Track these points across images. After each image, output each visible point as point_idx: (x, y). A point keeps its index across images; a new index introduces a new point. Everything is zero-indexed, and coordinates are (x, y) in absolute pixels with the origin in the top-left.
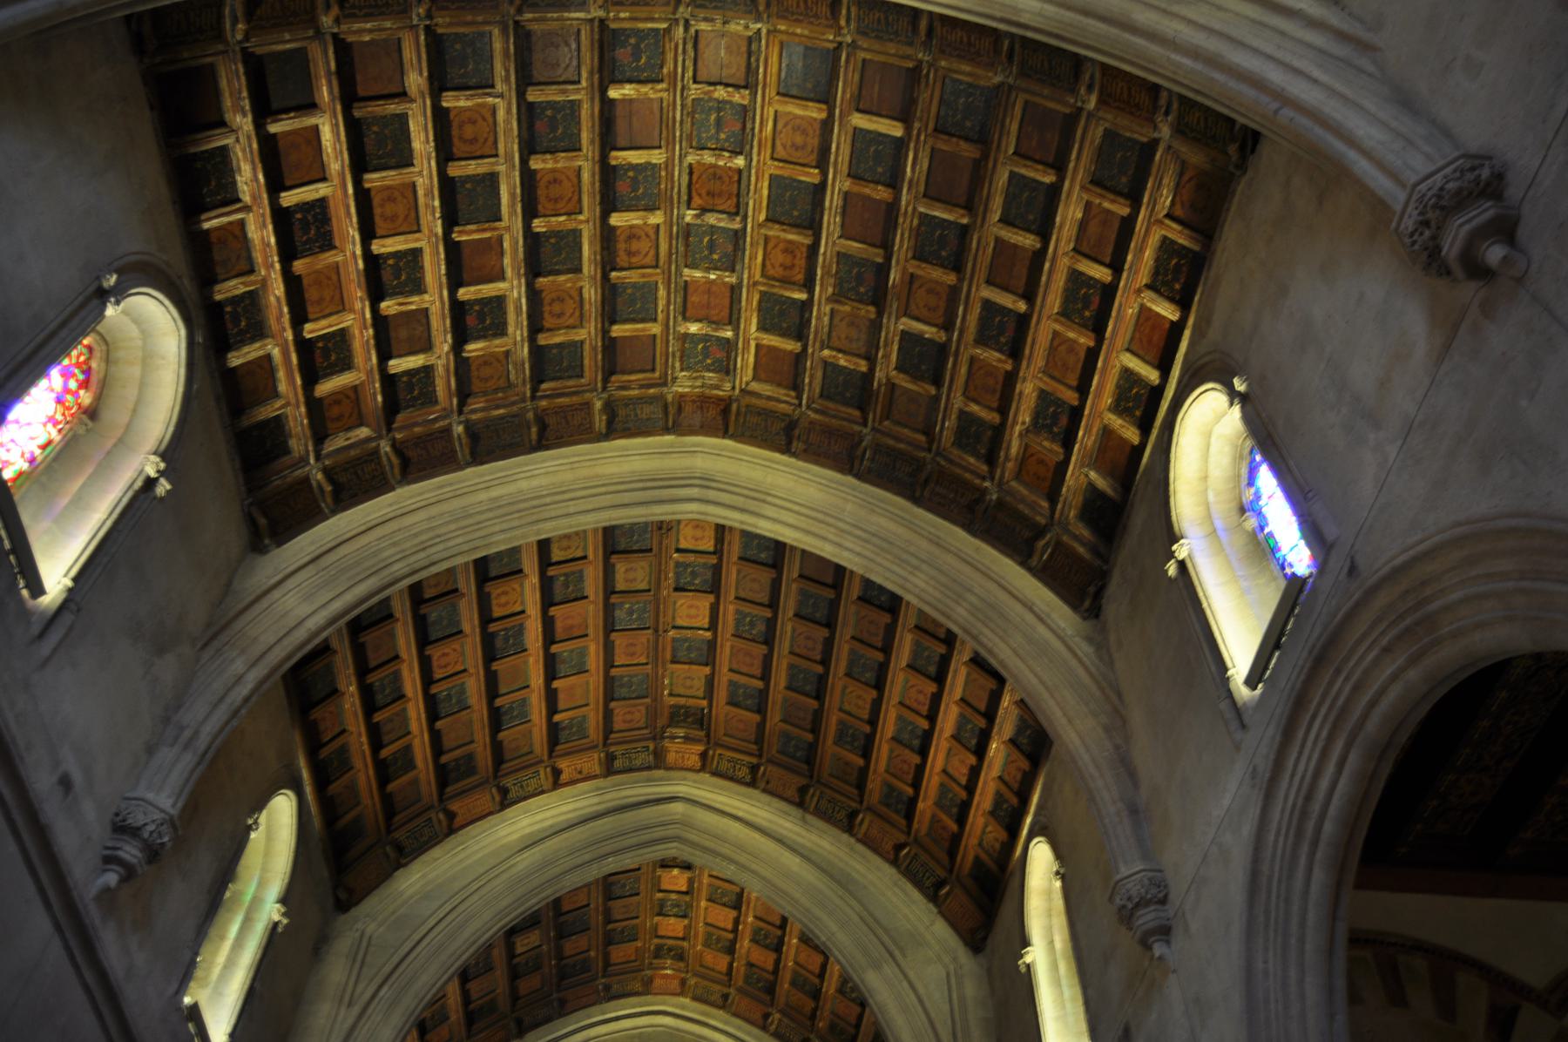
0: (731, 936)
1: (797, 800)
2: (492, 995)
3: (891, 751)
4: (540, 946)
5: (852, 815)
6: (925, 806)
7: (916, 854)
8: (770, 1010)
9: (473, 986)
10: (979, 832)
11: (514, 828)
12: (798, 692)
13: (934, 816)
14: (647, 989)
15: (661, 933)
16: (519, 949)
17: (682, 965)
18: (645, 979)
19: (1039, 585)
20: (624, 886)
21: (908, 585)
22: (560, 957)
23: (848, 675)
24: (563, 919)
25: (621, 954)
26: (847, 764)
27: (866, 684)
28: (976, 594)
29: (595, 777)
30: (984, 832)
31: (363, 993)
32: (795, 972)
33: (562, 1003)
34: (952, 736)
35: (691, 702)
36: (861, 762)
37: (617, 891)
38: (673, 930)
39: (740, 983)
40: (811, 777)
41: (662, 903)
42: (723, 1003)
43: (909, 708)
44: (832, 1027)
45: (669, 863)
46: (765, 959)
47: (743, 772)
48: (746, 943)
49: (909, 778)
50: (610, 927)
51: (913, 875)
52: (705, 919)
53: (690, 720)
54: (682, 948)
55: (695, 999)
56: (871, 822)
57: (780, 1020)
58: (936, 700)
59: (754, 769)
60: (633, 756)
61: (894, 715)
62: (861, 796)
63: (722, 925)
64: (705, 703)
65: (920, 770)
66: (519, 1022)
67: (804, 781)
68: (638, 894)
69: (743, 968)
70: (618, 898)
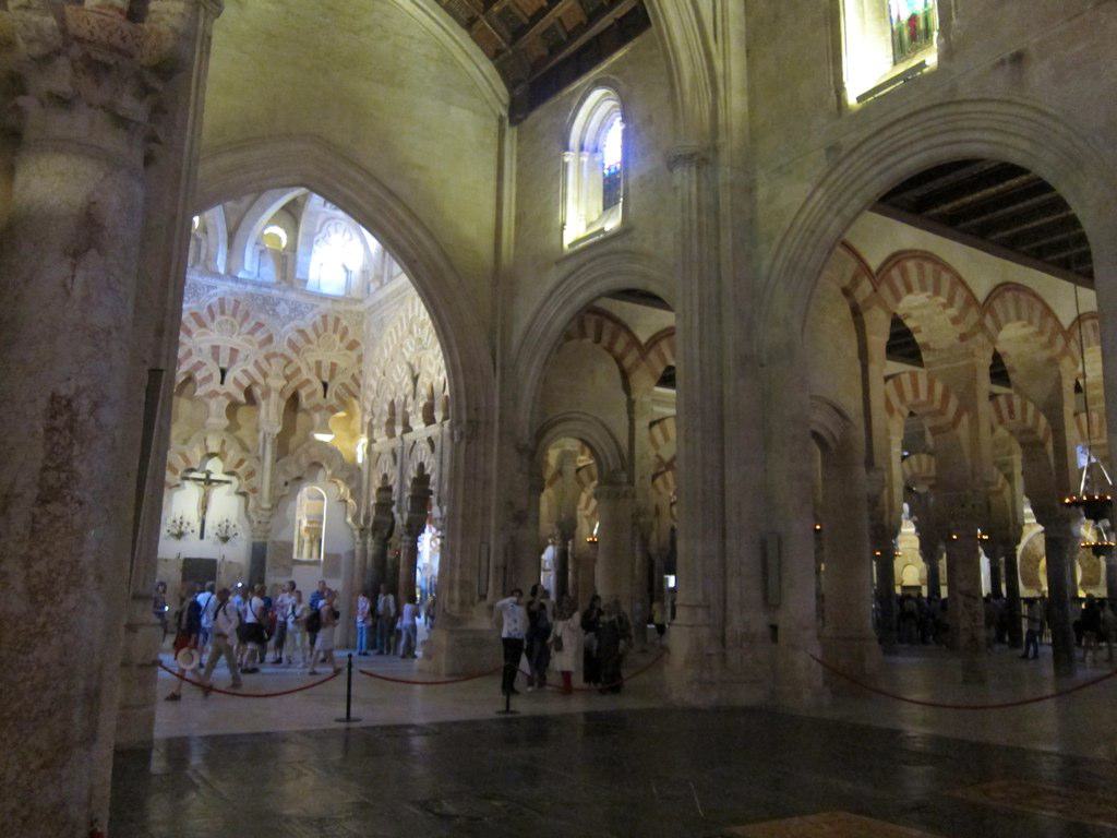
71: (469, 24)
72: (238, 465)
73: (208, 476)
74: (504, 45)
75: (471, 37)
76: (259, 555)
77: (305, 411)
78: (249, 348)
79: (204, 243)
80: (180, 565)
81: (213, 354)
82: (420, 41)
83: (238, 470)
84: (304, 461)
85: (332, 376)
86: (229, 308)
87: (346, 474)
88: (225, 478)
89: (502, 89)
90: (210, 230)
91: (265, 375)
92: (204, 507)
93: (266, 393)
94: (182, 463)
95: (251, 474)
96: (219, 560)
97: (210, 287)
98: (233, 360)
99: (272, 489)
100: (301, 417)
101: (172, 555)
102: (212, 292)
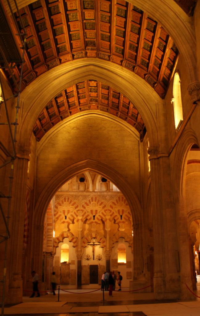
0: (108, 96)
1: (120, 64)
3: (143, 51)
4: (63, 101)
5: (134, 67)
6: (151, 65)
7: (149, 76)
8: (118, 112)
10: (164, 71)
12: (119, 36)
13: (153, 67)
14: (90, 108)
15: (91, 96)
17: (97, 103)
19: (178, 6)
20: (81, 86)
21: (143, 7)
23: (131, 31)
26: (132, 54)
27: (136, 33)
28: (162, 10)
29: (70, 60)
30: (165, 71)
31: (24, 114)
32: (123, 103)
33: (70, 112)
34: (158, 47)
35: (92, 40)
36: (135, 54)
37: (79, 87)
39: (111, 106)
40: (124, 58)
41: (91, 89)
42: (107, 111)
43: (147, 40)
44: (132, 115)
47: (107, 57)
48: (111, 97)
49: (147, 58)
50: (79, 95)
51: (149, 82)
53: (92, 44)
54: (97, 99)
55: (101, 110)
56: (138, 69)
57: (120, 114)
58: (153, 37)
59: (109, 56)
60: (79, 55)
61: (143, 42)
62: (136, 62)
64: (95, 40)
65: (150, 56)
66: (61, 117)
67: (122, 59)
68: (85, 87)
69: (111, 103)
71: (125, 119)
72: (100, 240)
73: (94, 244)
74: (135, 122)
75: (128, 122)
76: (108, 262)
78: (99, 208)
79: (87, 185)
80: (89, 267)
82: (115, 127)
83: (100, 241)
86: (94, 199)
89: (137, 133)
90: (87, 181)
91: (105, 216)
93: (106, 220)
94: (86, 240)
95: (104, 242)
97: (89, 195)
98: (96, 213)
101: (86, 264)
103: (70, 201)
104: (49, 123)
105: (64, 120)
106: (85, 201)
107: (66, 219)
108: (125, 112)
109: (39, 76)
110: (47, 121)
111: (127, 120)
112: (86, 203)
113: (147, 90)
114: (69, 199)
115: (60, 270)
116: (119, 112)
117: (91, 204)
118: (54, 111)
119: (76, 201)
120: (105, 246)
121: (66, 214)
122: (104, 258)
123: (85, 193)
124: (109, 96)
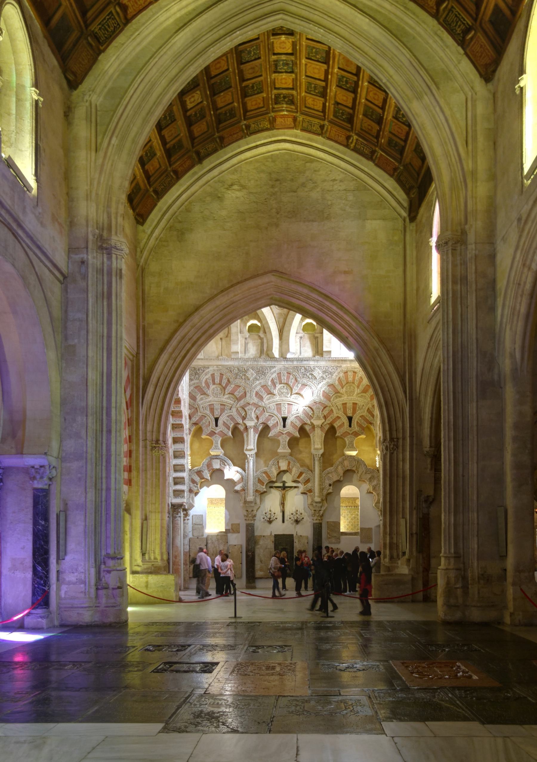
0: (323, 84)
2: (179, 138)
4: (202, 102)
8: (351, 134)
9: (165, 132)
11: (168, 14)
16: (189, 106)
18: (271, 118)
22: (216, 109)
24: (213, 81)
25: (254, 103)
32: (366, 105)
33: (222, 139)
37: (245, 57)
38: (286, 83)
44: (390, 142)
45: (279, 32)
46: (346, 98)
48: (334, 88)
52: (306, 72)
57: (357, 140)
63: (317, 76)
66: (198, 153)
70: (248, 62)
71: (370, 157)
72: (299, 477)
73: (284, 485)
75: (377, 165)
77: (338, 437)
80: (273, 539)
81: (277, 409)
83: (300, 480)
84: (341, 471)
85: (354, 410)
87: (369, 476)
88: (294, 485)
92: (283, 504)
95: (307, 481)
96: (295, 535)
99: (321, 490)
100: (339, 442)
102: (273, 370)
103: (224, 382)
104: (167, 170)
105: (206, 162)
106: (262, 381)
107: (217, 425)
108: (369, 134)
109: (134, 21)
110: (160, 166)
111: (374, 158)
112: (264, 387)
113: (442, 54)
114: (224, 377)
115: (206, 545)
116: (353, 135)
117: (277, 388)
118: (179, 135)
119: (238, 381)
120: (310, 491)
121: (217, 413)
122: (309, 520)
123: (262, 363)
124: (327, 85)
